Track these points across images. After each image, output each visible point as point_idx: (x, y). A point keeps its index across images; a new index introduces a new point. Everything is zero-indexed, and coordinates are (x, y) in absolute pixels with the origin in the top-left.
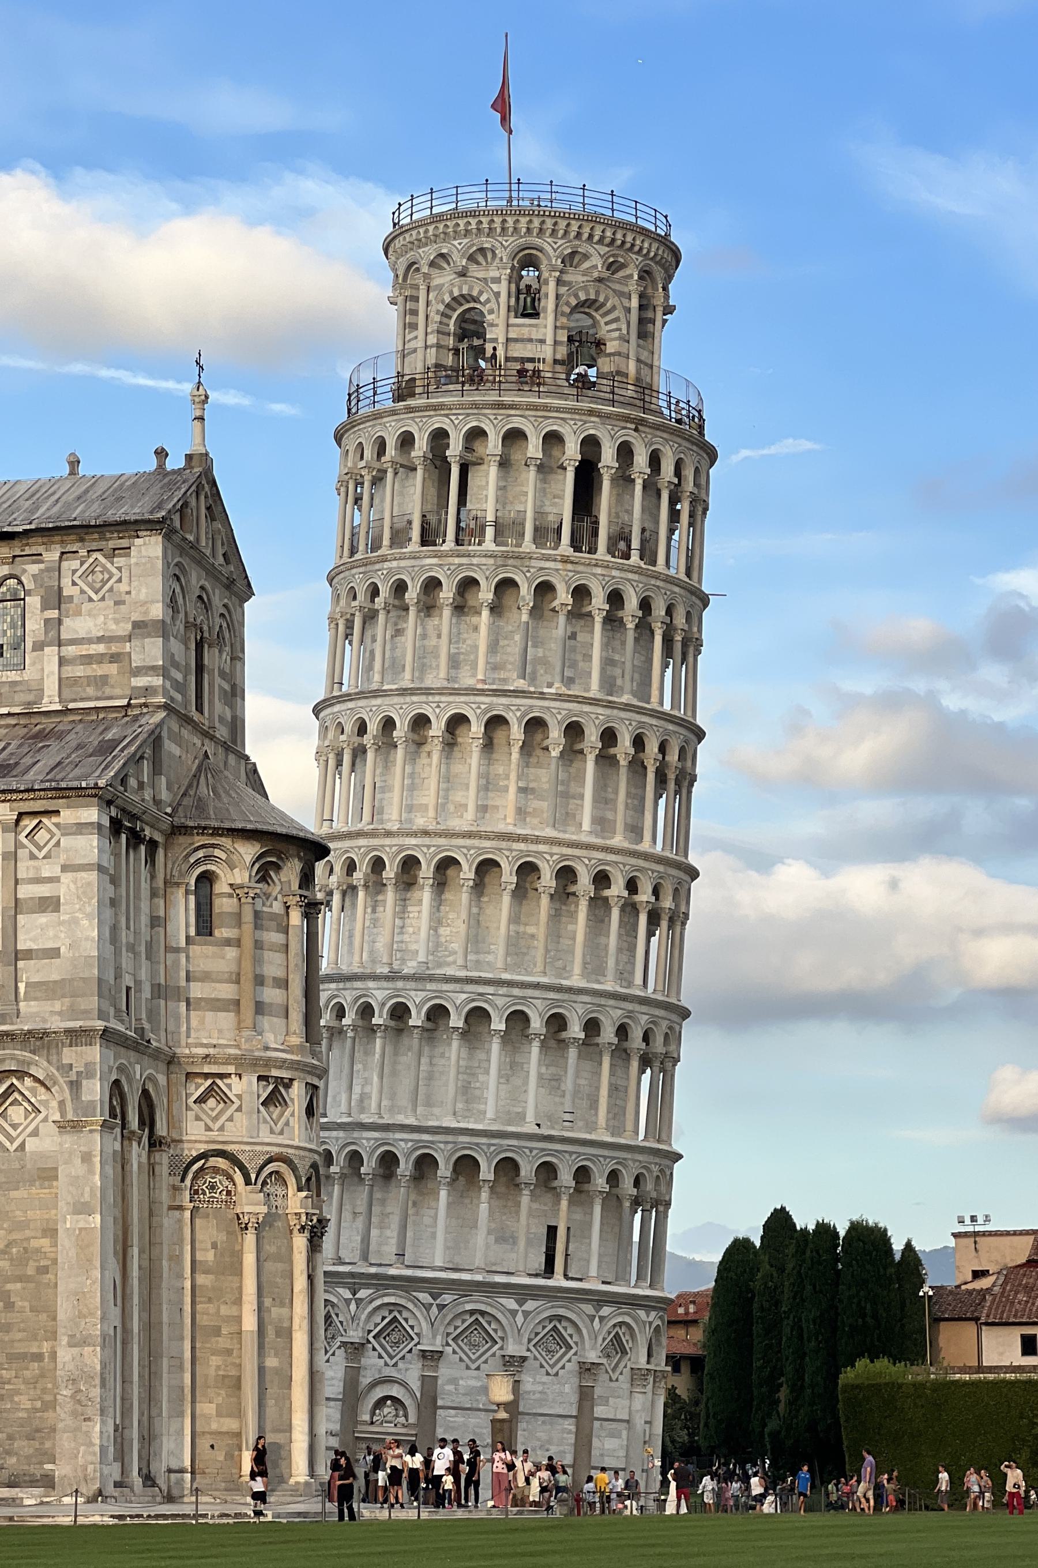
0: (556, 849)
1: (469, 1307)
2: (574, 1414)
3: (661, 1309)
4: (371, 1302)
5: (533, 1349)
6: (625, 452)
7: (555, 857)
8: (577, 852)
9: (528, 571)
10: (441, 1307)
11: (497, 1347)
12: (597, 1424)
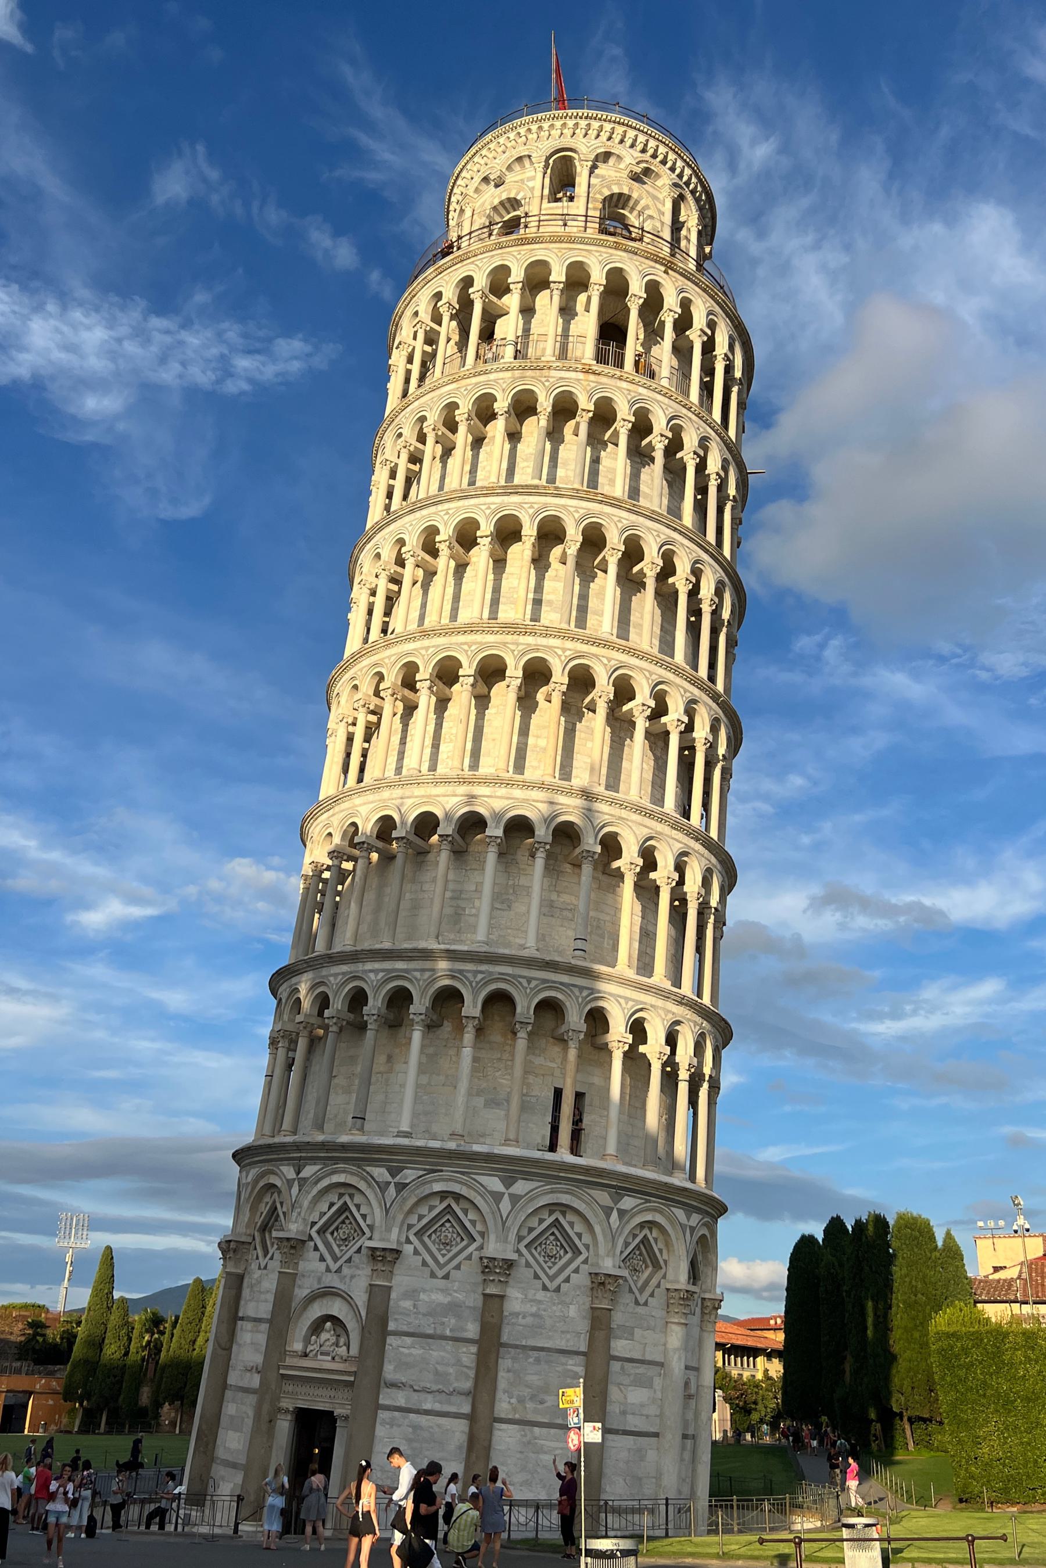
0: (569, 644)
1: (437, 1187)
2: (583, 1348)
3: (708, 1213)
4: (316, 1183)
5: (524, 1251)
7: (568, 653)
8: (594, 650)
9: (548, 381)
10: (401, 1187)
11: (474, 1246)
12: (616, 1366)
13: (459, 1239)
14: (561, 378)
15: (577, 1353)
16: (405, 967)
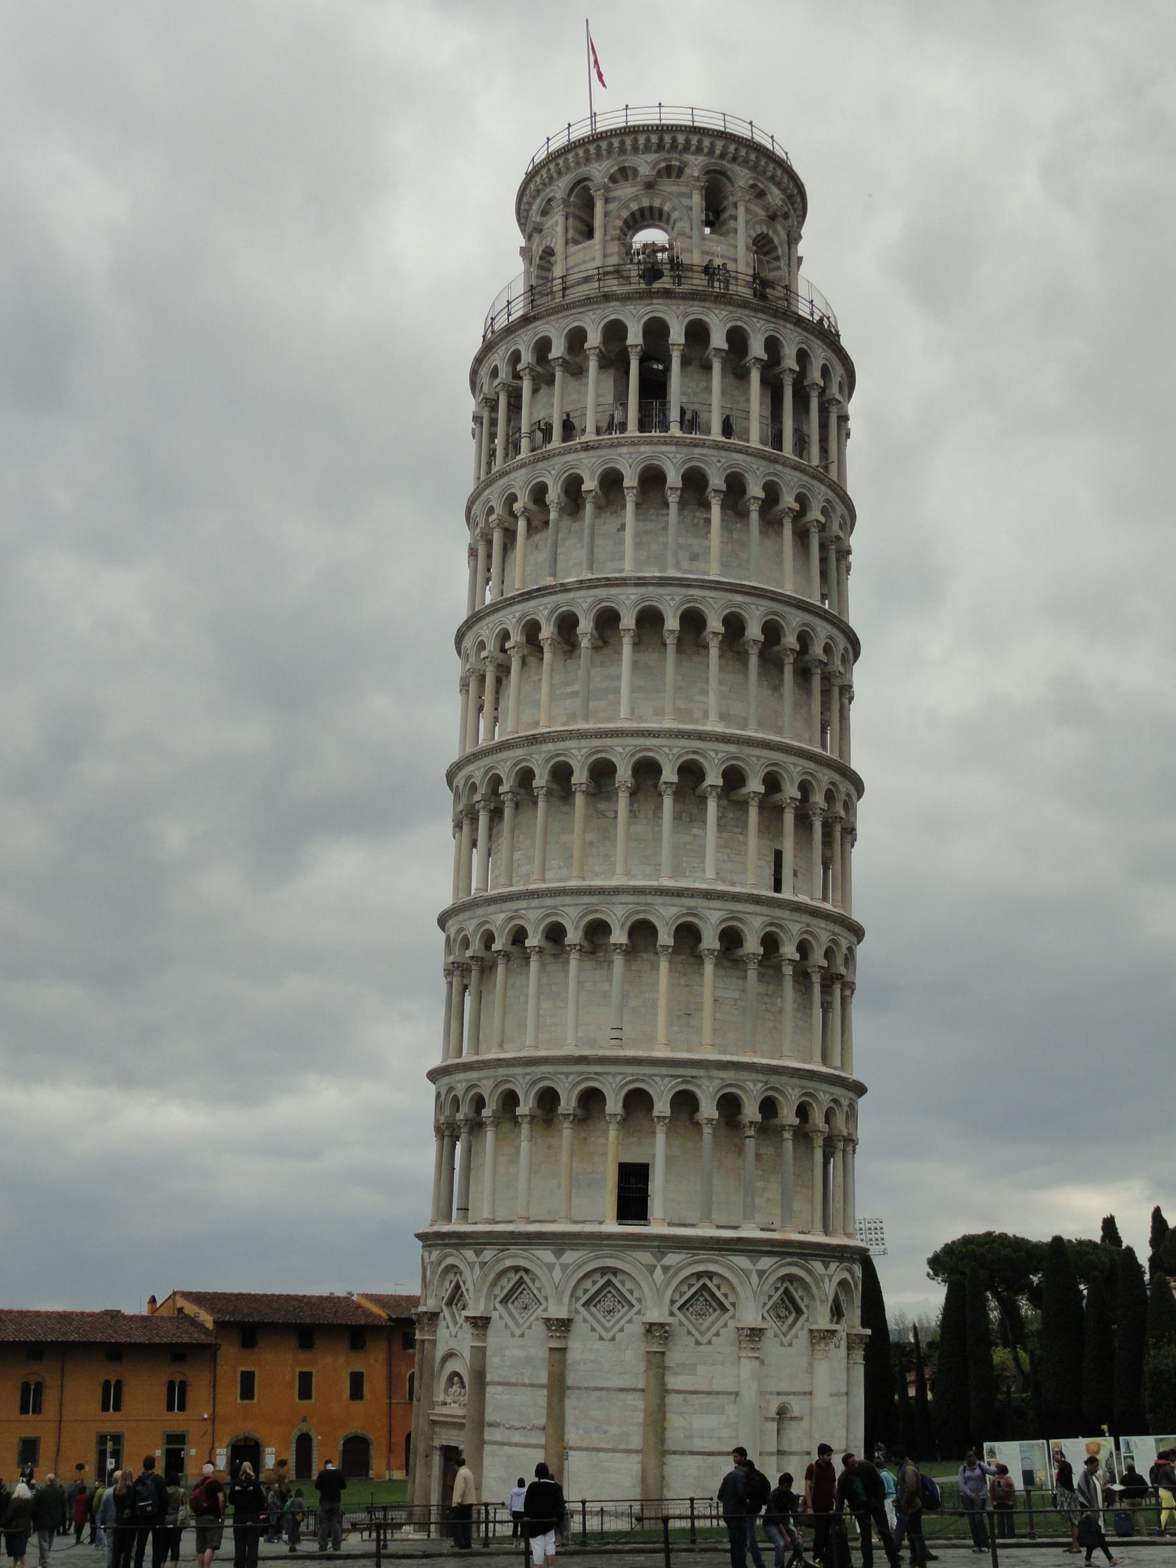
0: (585, 743)
1: (509, 1263)
2: (641, 1385)
6: (656, 330)
7: (584, 751)
8: (608, 742)
9: (554, 469)
11: (541, 1308)
13: (533, 1304)
14: (566, 462)
15: (635, 1390)
16: (478, 1076)
